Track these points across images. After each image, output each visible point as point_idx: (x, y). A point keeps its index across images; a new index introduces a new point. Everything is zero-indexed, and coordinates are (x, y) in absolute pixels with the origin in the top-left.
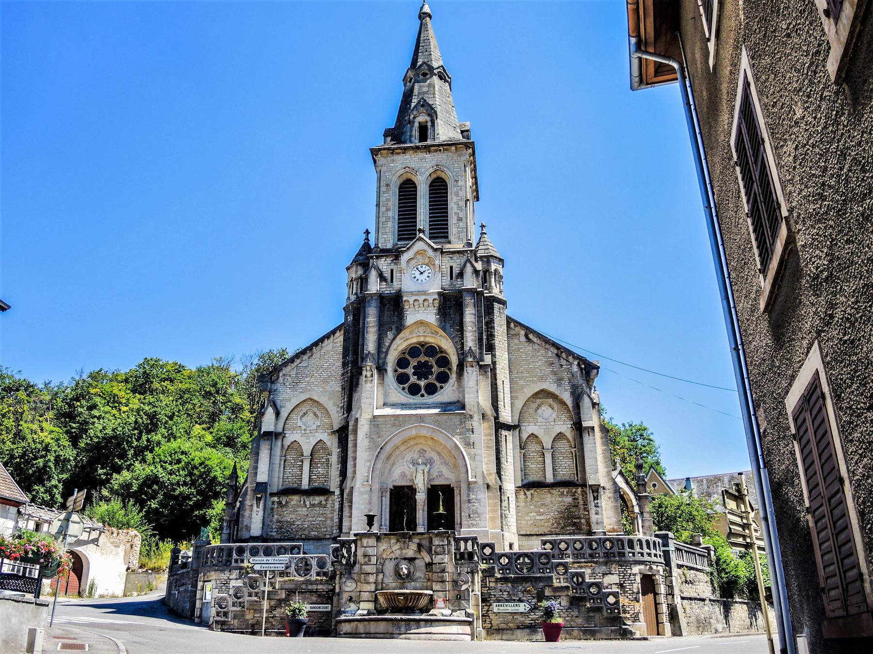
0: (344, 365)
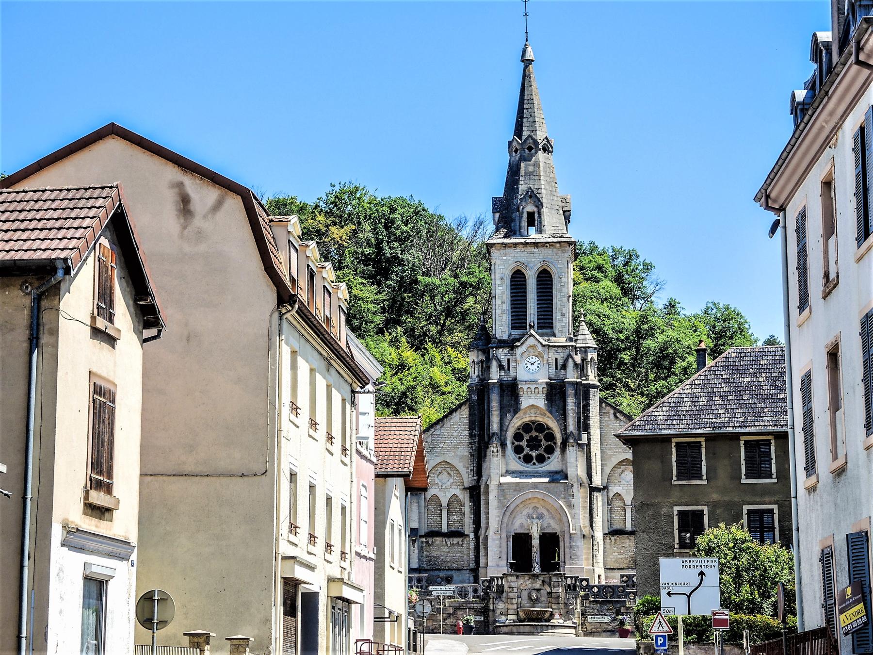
0: (471, 436)
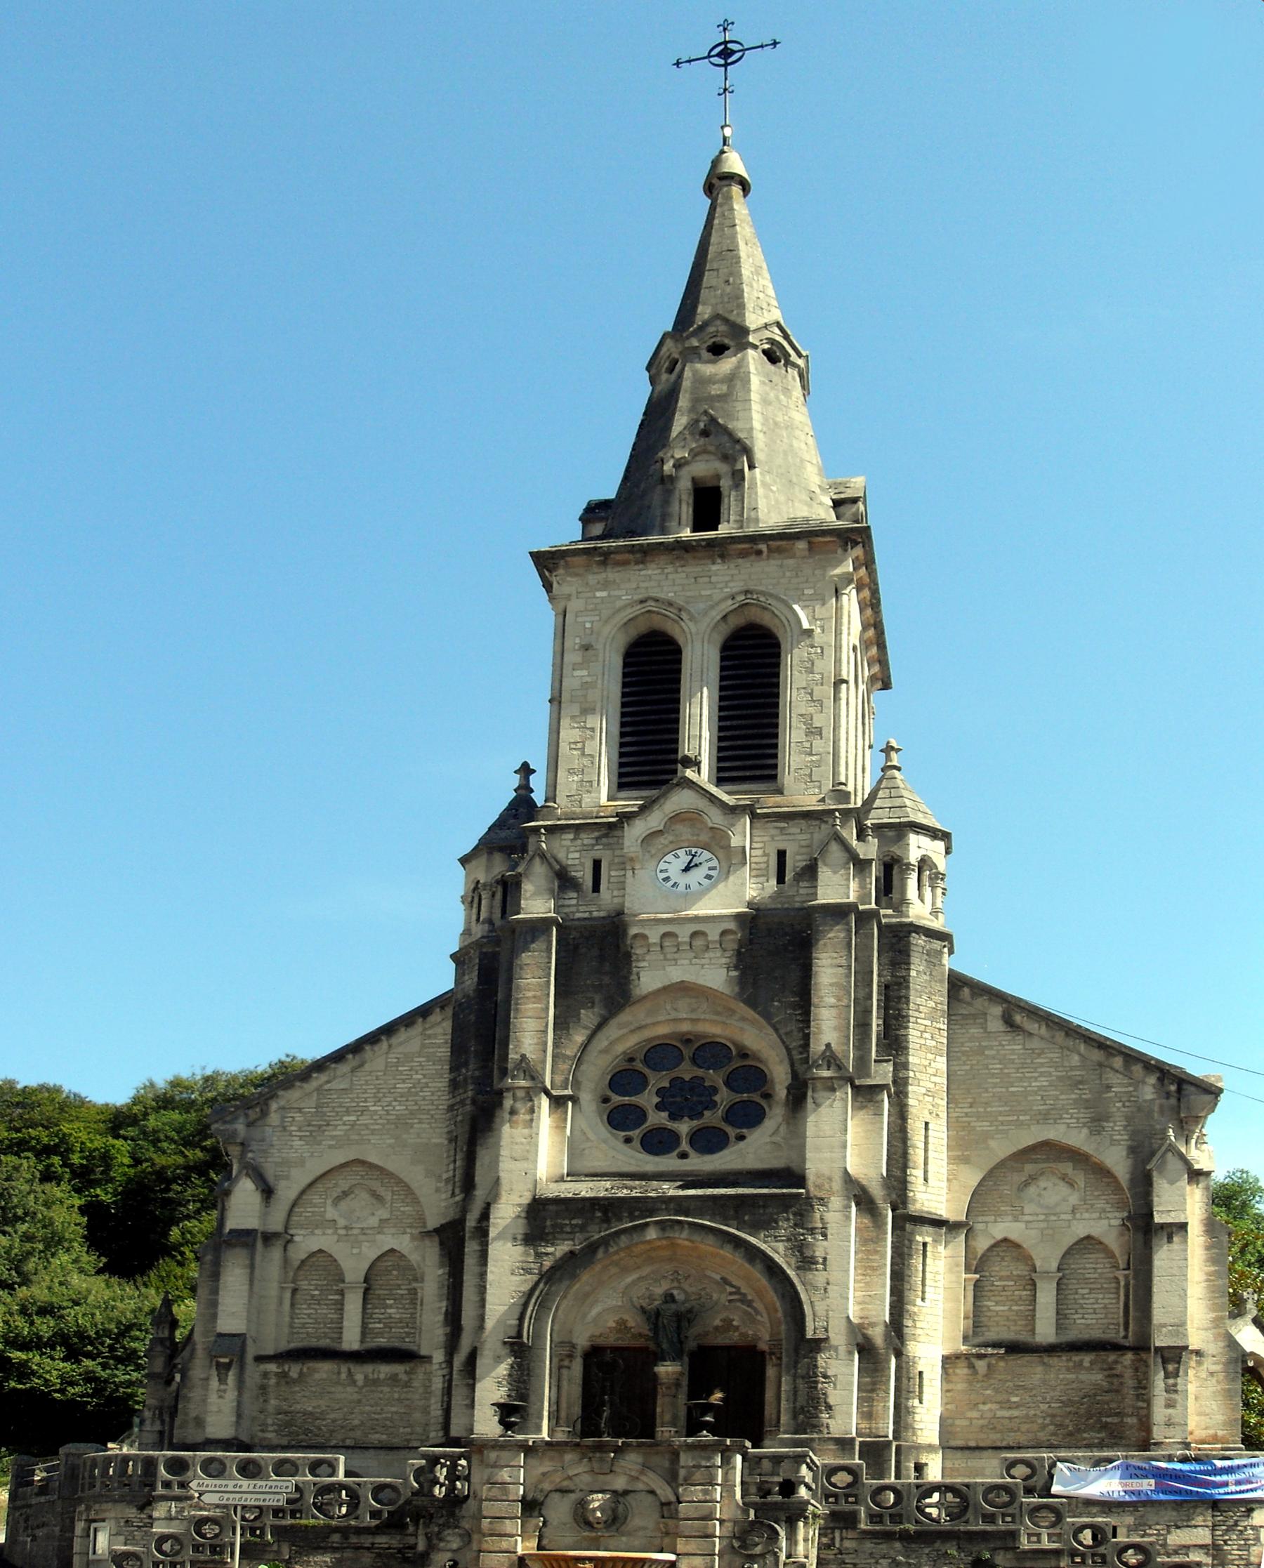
0: (454, 1085)
